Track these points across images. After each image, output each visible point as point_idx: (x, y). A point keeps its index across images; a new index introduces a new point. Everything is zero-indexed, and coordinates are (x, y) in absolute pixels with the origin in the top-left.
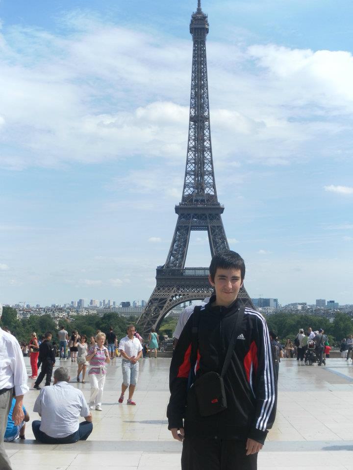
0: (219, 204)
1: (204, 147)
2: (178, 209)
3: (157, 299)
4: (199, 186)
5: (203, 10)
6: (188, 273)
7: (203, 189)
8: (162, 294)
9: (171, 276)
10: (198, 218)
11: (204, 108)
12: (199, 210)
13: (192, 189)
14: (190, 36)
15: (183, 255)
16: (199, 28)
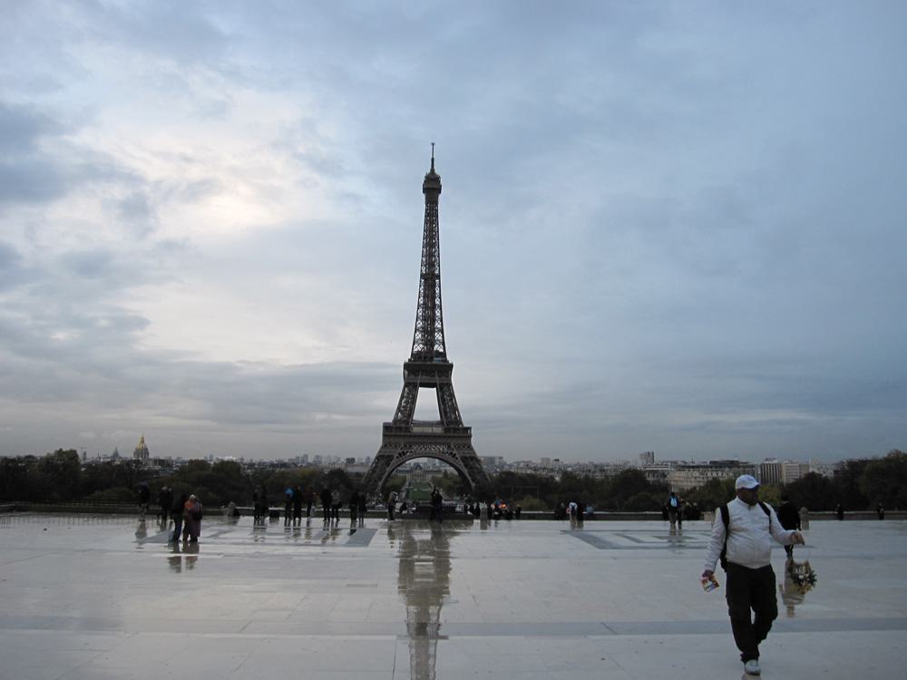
0: (446, 361)
1: (434, 305)
3: (383, 456)
5: (436, 171)
6: (416, 430)
7: (433, 346)
8: (388, 452)
9: (400, 431)
10: (426, 375)
11: (434, 266)
12: (428, 367)
13: (421, 345)
14: (423, 196)
16: (432, 187)
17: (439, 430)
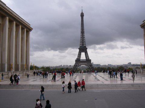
2: (79, 49)
4: (83, 45)
9: (78, 61)
15: (80, 57)
16: (82, 15)
17: (85, 60)
